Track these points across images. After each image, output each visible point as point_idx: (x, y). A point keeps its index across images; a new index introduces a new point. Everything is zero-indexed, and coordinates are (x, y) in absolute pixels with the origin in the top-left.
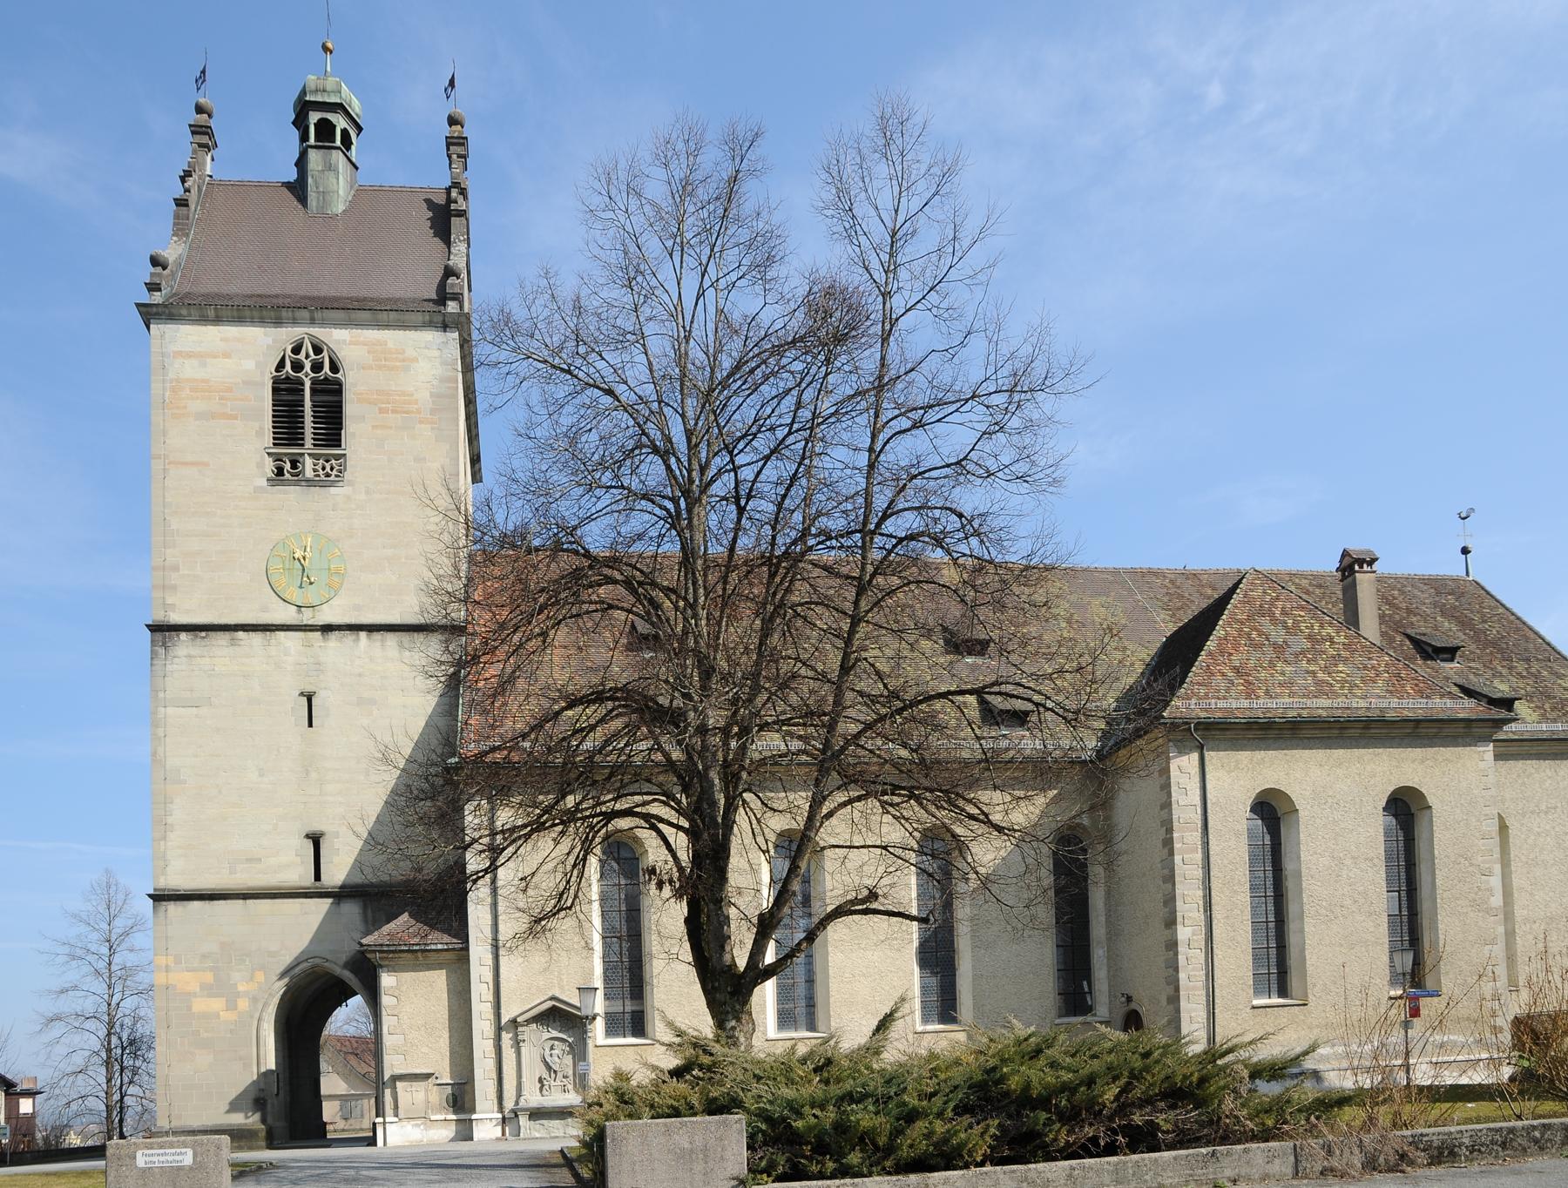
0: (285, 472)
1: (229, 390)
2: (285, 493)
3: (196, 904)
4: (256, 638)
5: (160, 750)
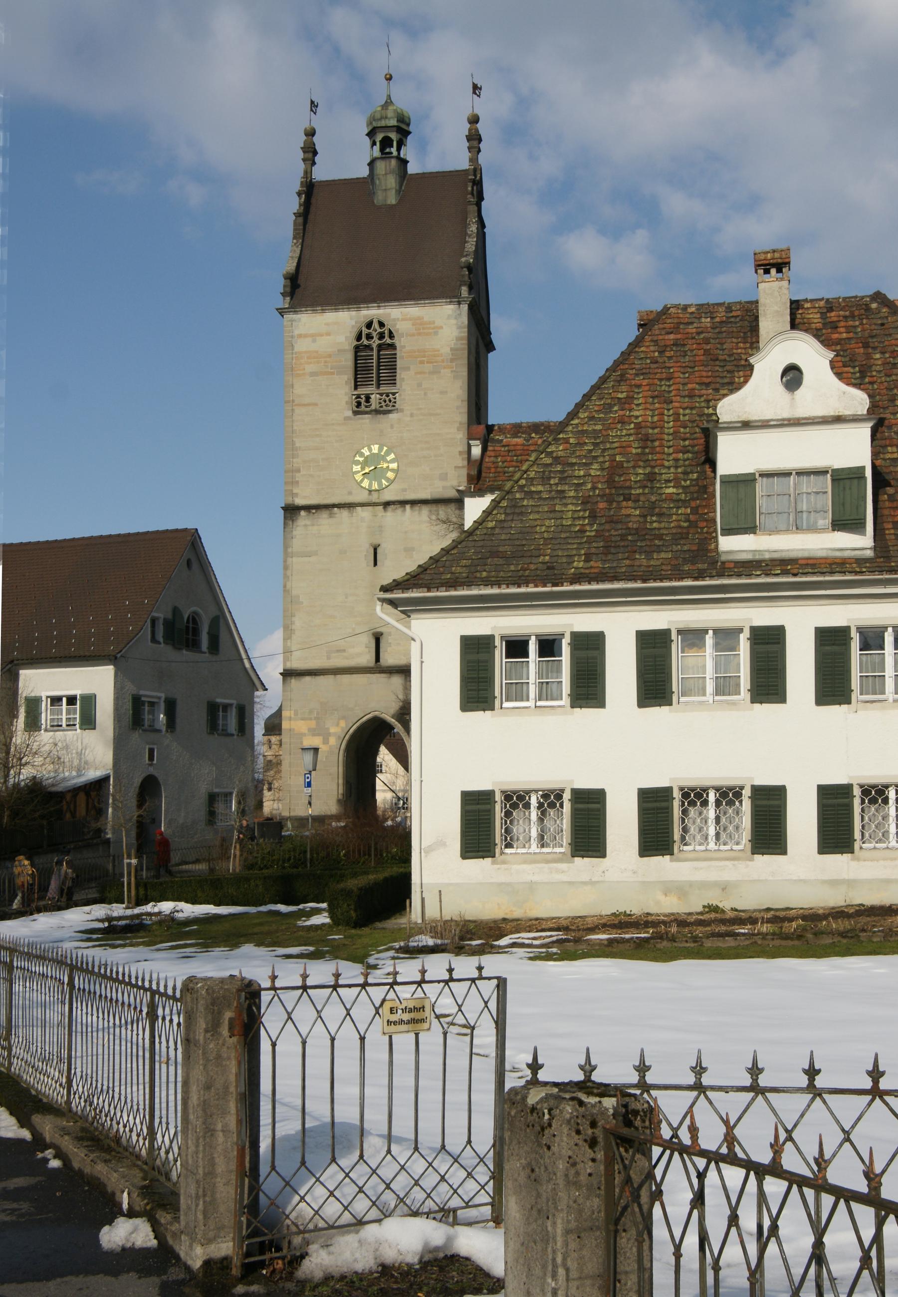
0: (361, 406)
1: (330, 356)
2: (363, 419)
3: (307, 679)
4: (345, 513)
5: (289, 585)
